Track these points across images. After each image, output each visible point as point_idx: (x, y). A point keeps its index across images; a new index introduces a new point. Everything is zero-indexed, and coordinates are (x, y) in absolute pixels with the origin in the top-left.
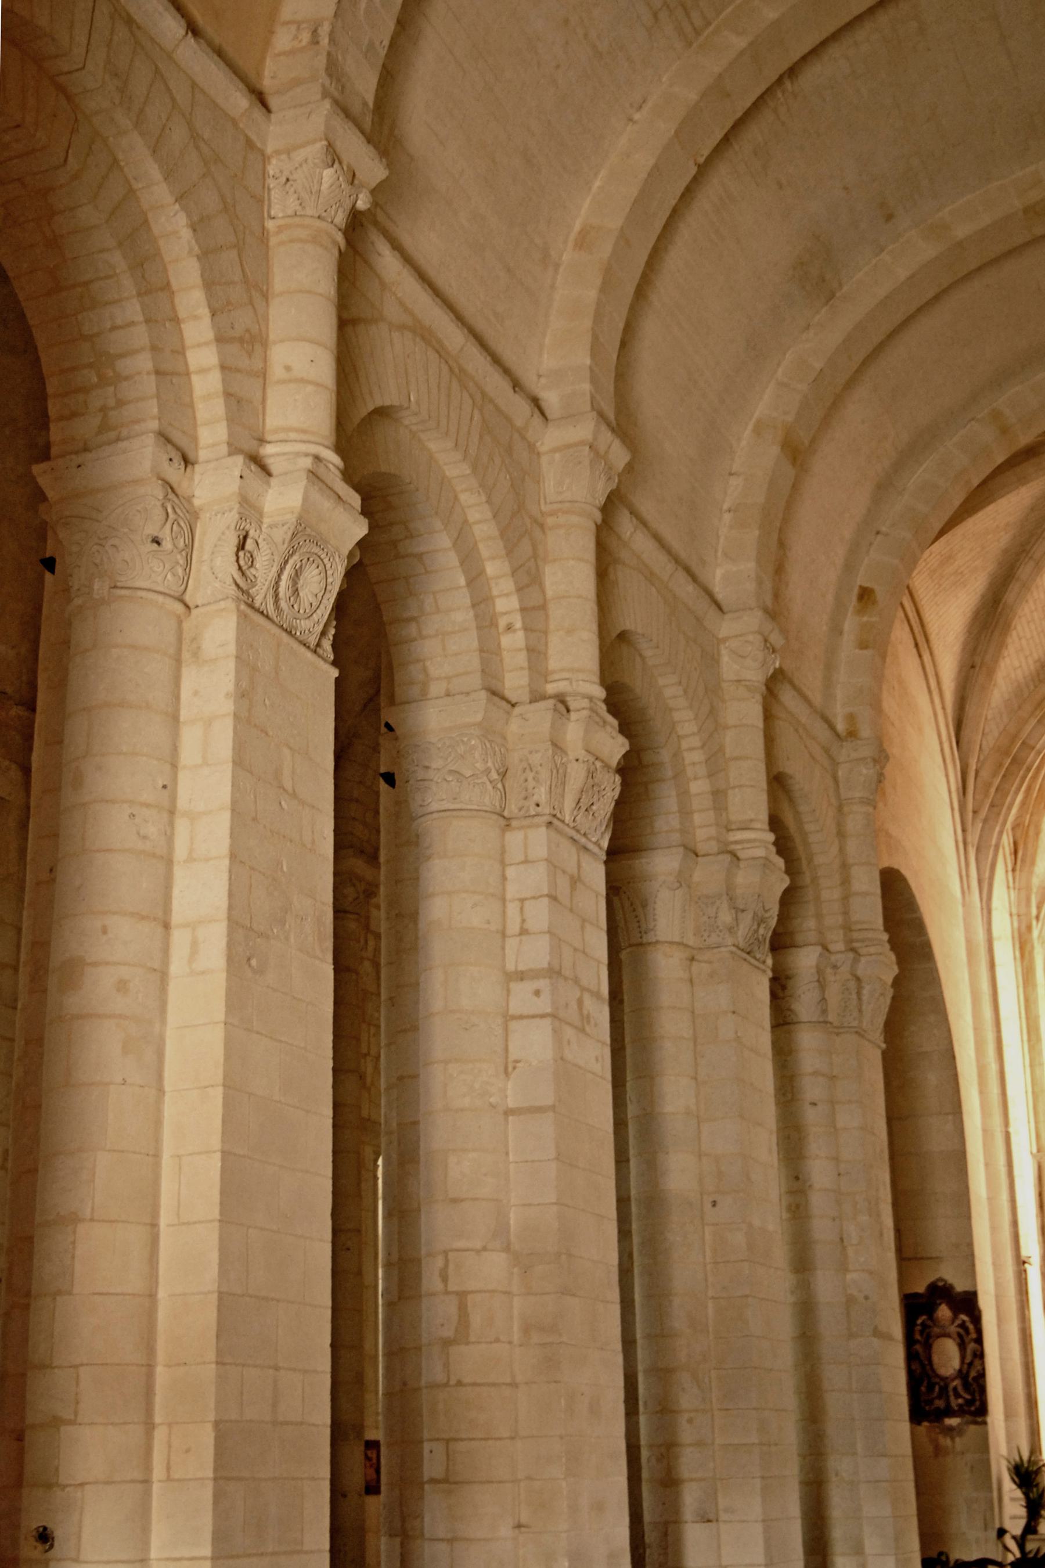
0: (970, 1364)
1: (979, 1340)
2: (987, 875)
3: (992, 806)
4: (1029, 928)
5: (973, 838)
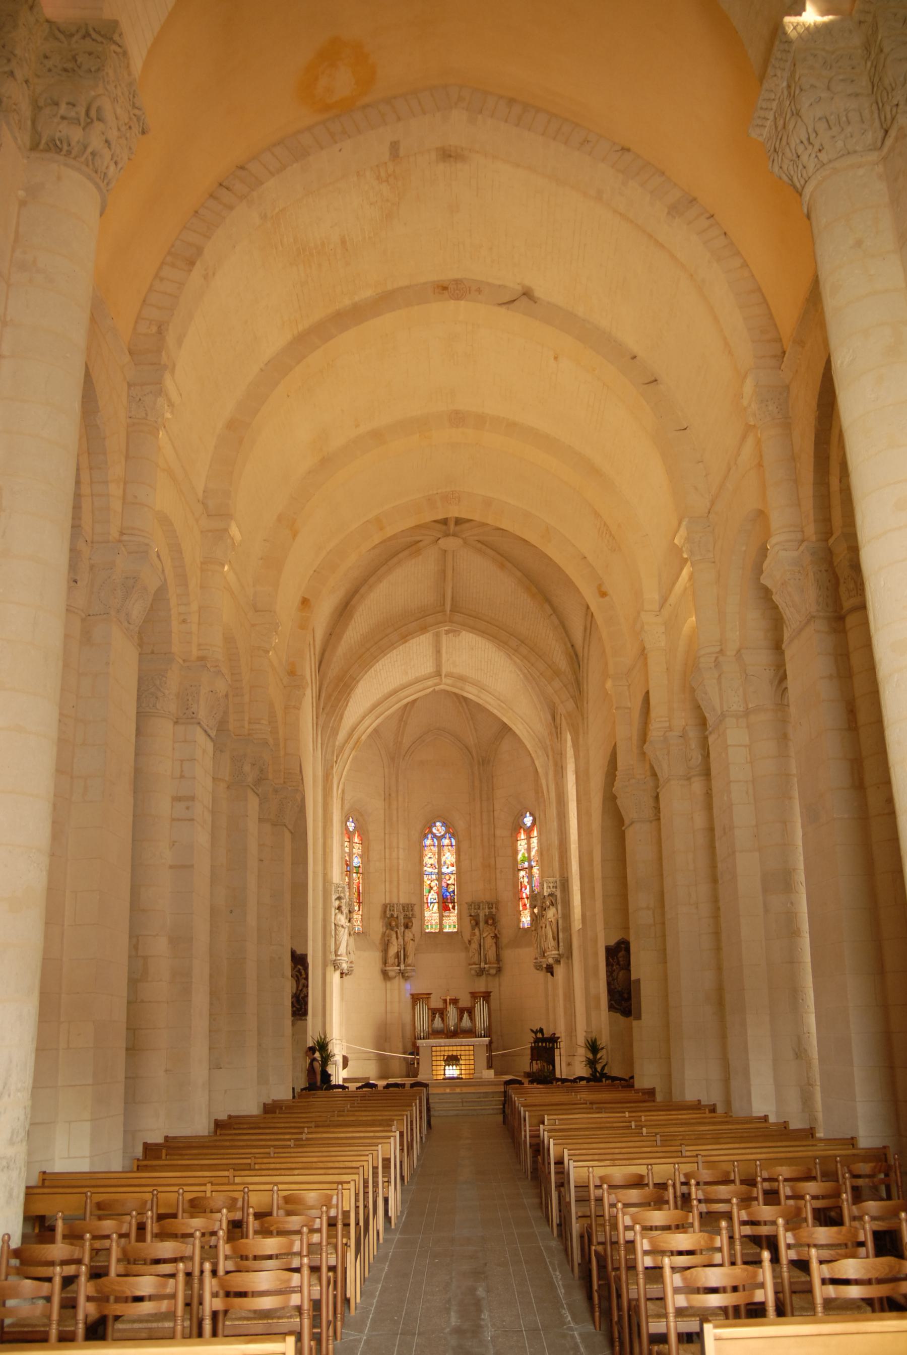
0: (301, 990)
1: (307, 979)
2: (326, 742)
3: (332, 706)
4: (332, 767)
5: (321, 723)
